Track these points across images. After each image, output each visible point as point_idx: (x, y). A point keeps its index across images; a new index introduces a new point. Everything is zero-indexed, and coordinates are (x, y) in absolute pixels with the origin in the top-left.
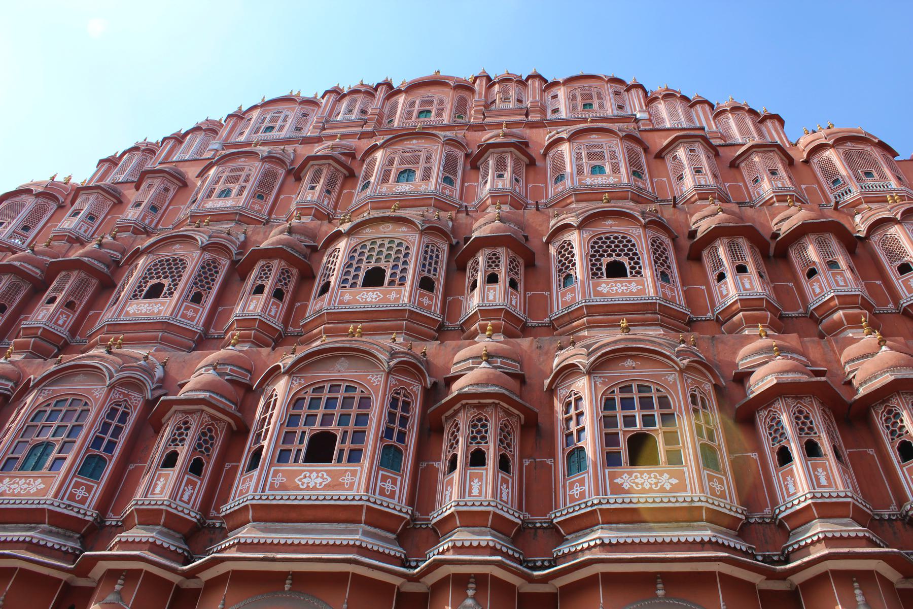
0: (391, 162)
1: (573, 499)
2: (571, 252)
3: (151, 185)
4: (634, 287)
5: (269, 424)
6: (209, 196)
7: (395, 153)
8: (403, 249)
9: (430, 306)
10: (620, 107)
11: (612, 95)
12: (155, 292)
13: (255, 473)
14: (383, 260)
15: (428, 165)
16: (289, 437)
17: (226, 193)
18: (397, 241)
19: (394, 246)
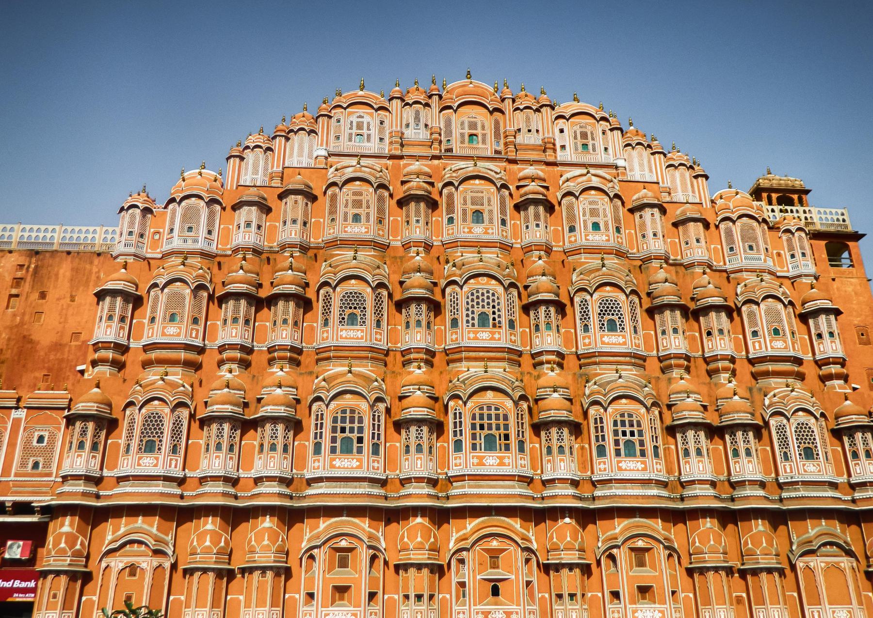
0: (465, 203)
1: (600, 470)
2: (587, 308)
3: (296, 202)
4: (621, 340)
5: (460, 426)
6: (346, 220)
8: (495, 298)
9: (515, 342)
10: (606, 149)
11: (601, 134)
12: (352, 320)
13: (461, 455)
14: (486, 307)
15: (490, 208)
16: (474, 437)
17: (356, 218)
18: (491, 292)
19: (490, 295)
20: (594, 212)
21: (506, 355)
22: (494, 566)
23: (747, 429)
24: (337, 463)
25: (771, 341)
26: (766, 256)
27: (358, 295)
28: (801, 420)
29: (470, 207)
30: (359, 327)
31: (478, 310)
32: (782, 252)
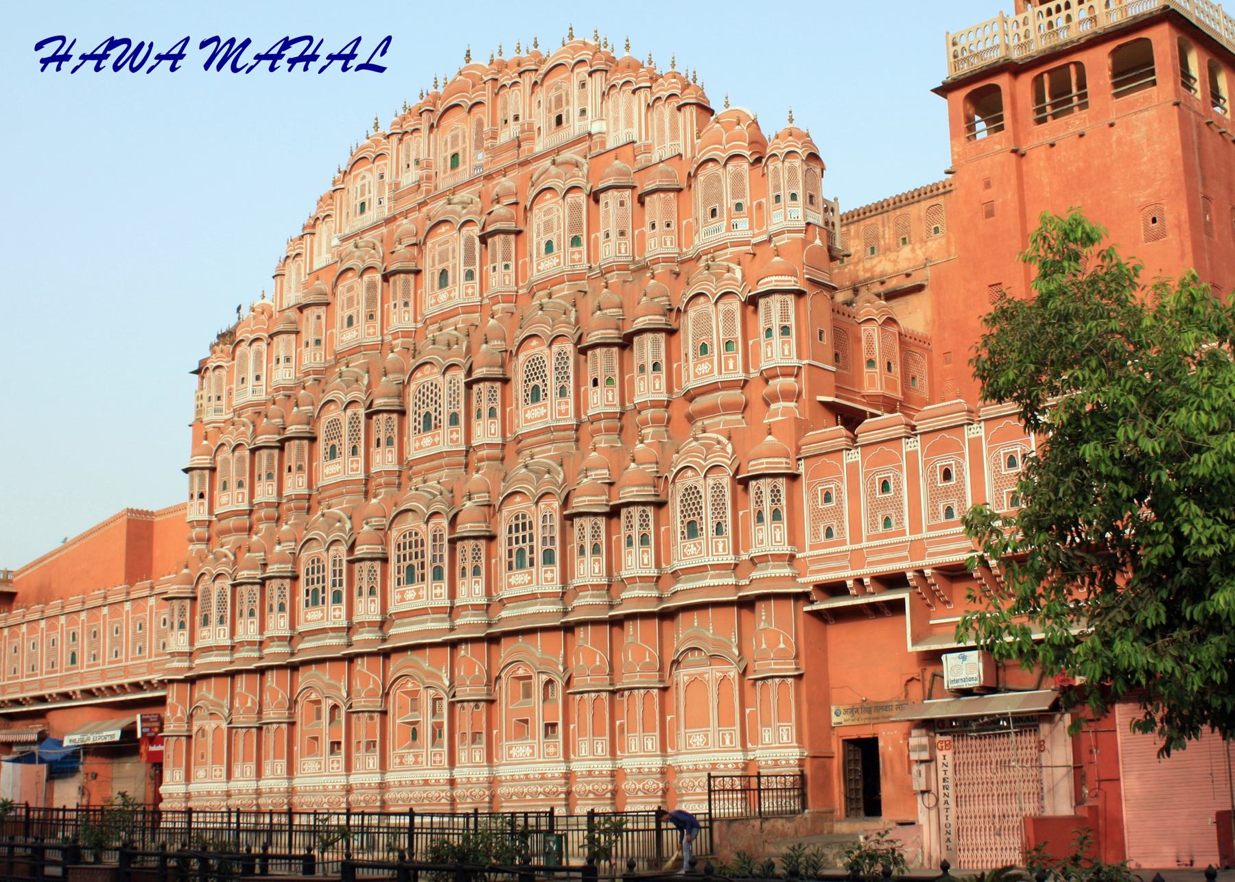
0: (434, 265)
4: (543, 411)
7: (433, 247)
10: (583, 112)
11: (576, 92)
20: (548, 227)
21: (443, 461)
22: (414, 710)
23: (631, 509)
24: (309, 617)
25: (695, 366)
26: (730, 218)
27: (335, 423)
28: (689, 483)
29: (440, 267)
30: (337, 460)
31: (423, 412)
32: (764, 200)
